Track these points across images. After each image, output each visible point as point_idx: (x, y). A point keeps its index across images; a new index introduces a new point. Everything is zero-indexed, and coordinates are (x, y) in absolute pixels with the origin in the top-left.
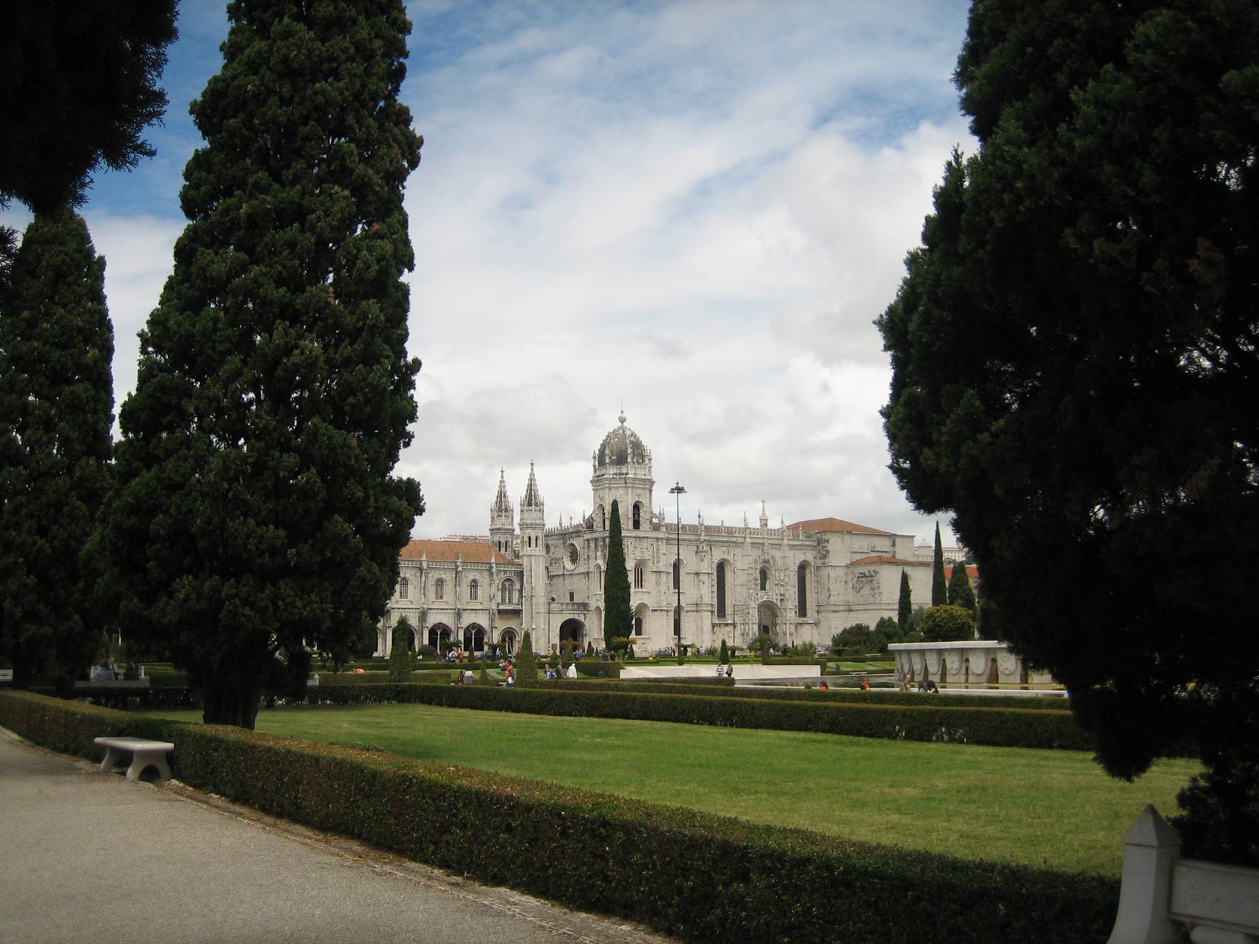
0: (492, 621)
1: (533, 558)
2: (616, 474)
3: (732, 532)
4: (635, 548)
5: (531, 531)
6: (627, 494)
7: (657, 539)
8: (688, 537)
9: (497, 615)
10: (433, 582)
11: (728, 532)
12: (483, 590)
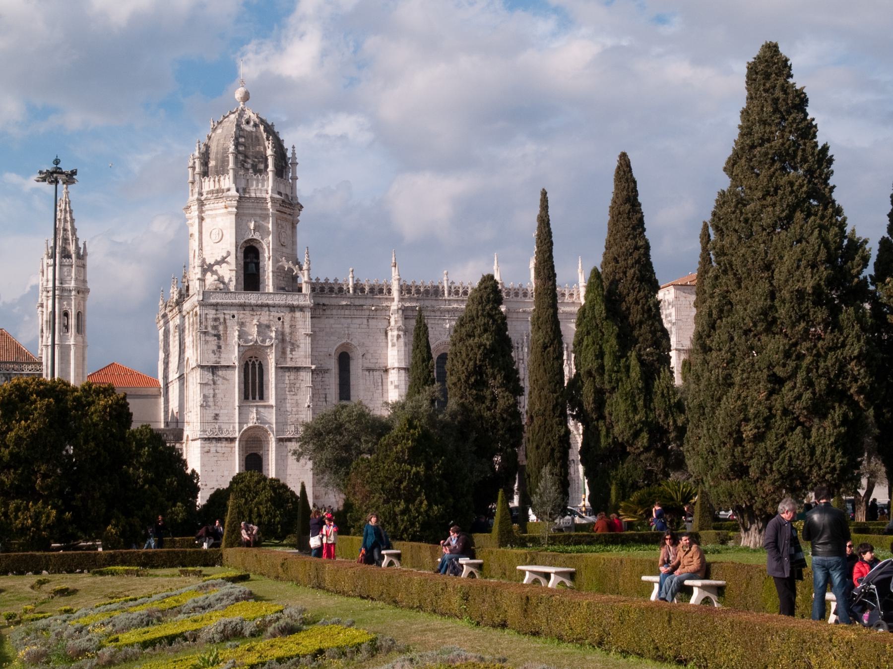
2: (211, 192)
4: (242, 324)
7: (292, 308)
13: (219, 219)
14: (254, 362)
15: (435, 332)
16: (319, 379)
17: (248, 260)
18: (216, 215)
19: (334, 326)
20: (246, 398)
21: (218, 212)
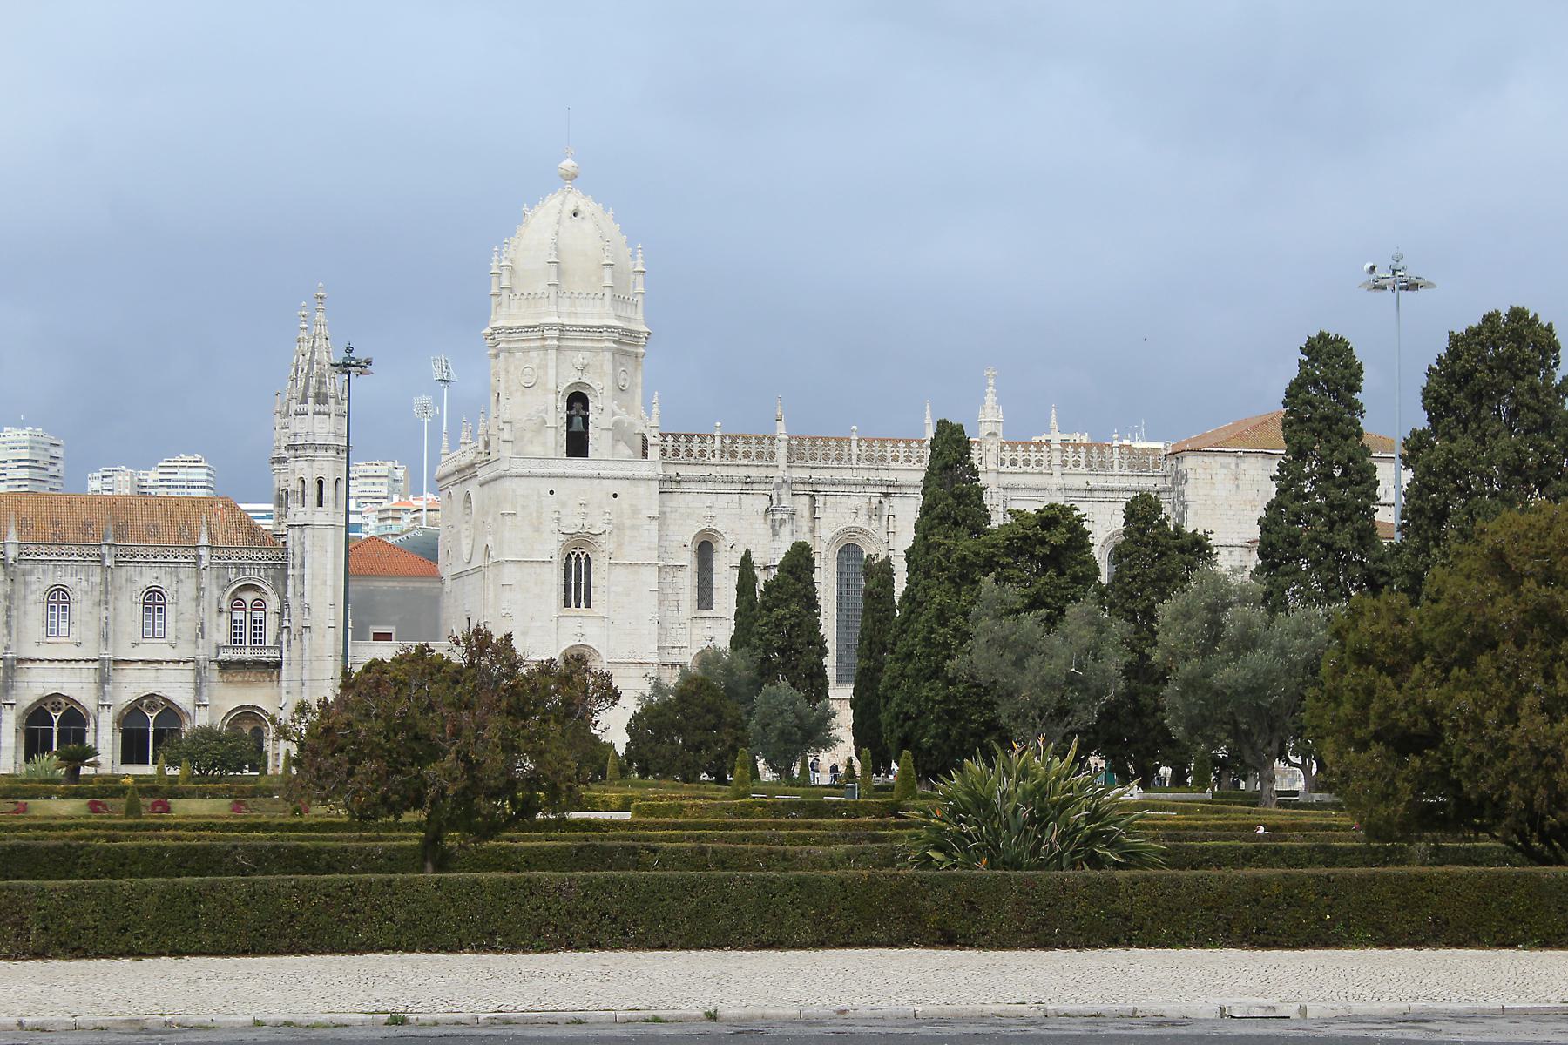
0: (198, 690)
1: (307, 530)
3: (883, 458)
5: (304, 464)
6: (544, 367)
8: (741, 473)
9: (214, 673)
10: (39, 596)
11: (869, 458)
12: (179, 614)
13: (533, 354)
14: (578, 555)
15: (837, 515)
16: (669, 579)
17: (572, 412)
18: (529, 349)
19: (691, 505)
20: (567, 605)
21: (532, 344)
